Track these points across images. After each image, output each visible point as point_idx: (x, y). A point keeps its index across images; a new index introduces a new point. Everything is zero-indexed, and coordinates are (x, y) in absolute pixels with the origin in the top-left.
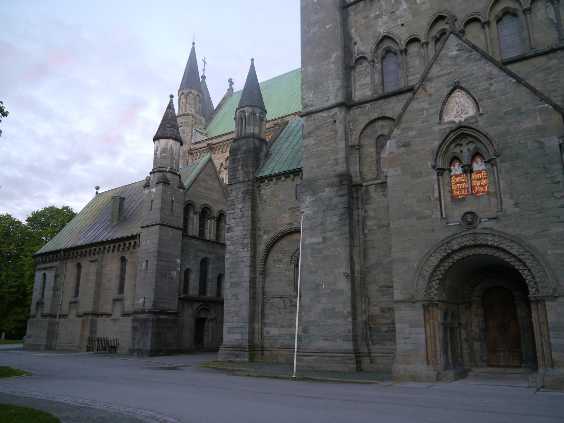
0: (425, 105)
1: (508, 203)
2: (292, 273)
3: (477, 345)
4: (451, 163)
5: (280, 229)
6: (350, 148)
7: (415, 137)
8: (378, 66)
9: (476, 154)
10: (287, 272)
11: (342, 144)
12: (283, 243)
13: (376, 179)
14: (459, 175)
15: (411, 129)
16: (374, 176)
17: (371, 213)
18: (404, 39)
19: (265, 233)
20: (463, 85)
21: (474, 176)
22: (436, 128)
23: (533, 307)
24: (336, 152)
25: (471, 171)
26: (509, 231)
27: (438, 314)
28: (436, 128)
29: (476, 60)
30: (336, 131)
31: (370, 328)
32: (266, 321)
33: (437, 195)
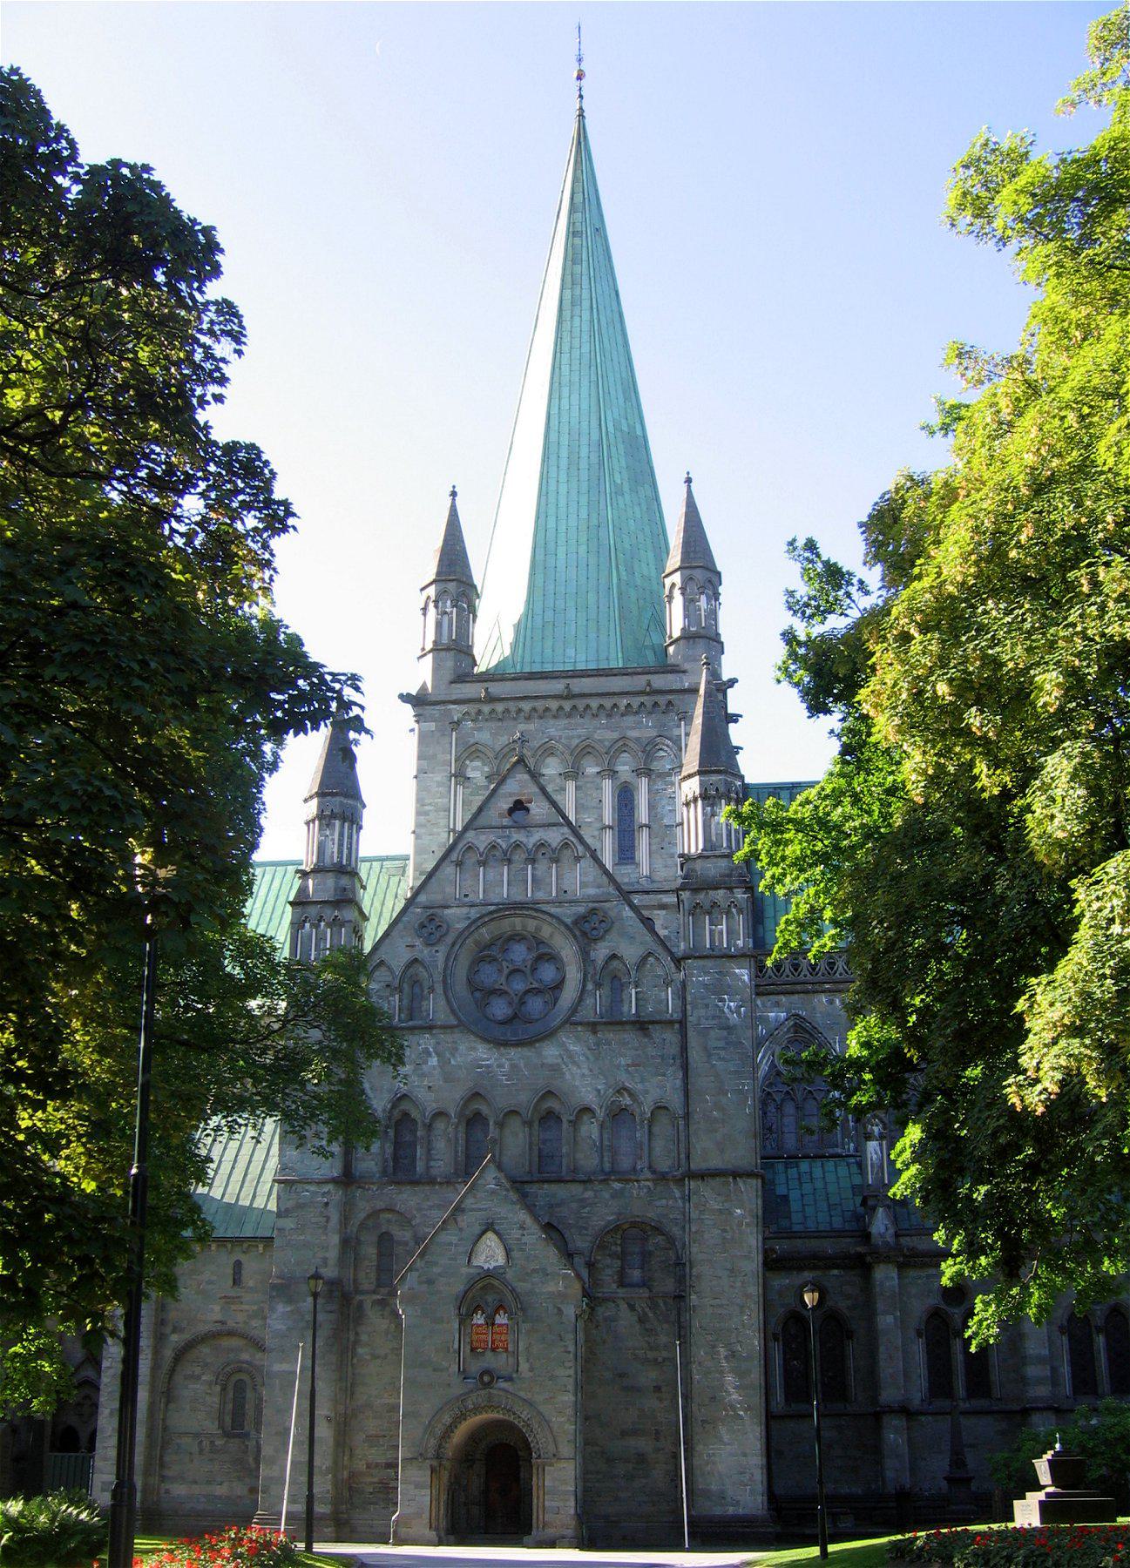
0: (454, 1239)
1: (524, 1366)
2: (217, 1400)
3: (475, 1510)
4: (475, 1311)
5: (203, 1328)
6: (345, 1242)
7: (440, 1275)
8: (391, 1132)
9: (500, 1307)
10: (208, 1398)
11: (335, 1239)
12: (205, 1350)
13: (374, 1292)
14: (481, 1325)
15: (435, 1264)
16: (372, 1287)
17: (364, 1338)
18: (429, 1109)
19: (174, 1331)
20: (497, 1228)
21: (496, 1329)
22: (464, 1270)
23: (534, 1471)
24: (325, 1248)
25: (493, 1324)
26: (522, 1394)
27: (445, 1475)
28: (464, 1270)
29: (513, 1203)
30: (328, 1219)
31: (350, 1488)
32: (167, 1473)
33: (456, 1346)
